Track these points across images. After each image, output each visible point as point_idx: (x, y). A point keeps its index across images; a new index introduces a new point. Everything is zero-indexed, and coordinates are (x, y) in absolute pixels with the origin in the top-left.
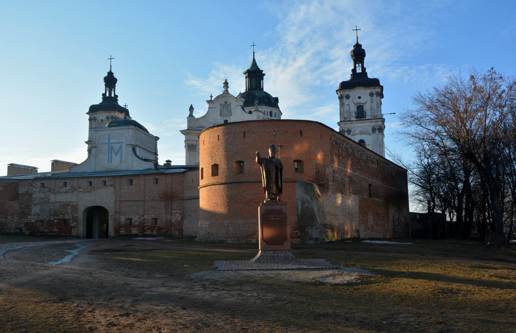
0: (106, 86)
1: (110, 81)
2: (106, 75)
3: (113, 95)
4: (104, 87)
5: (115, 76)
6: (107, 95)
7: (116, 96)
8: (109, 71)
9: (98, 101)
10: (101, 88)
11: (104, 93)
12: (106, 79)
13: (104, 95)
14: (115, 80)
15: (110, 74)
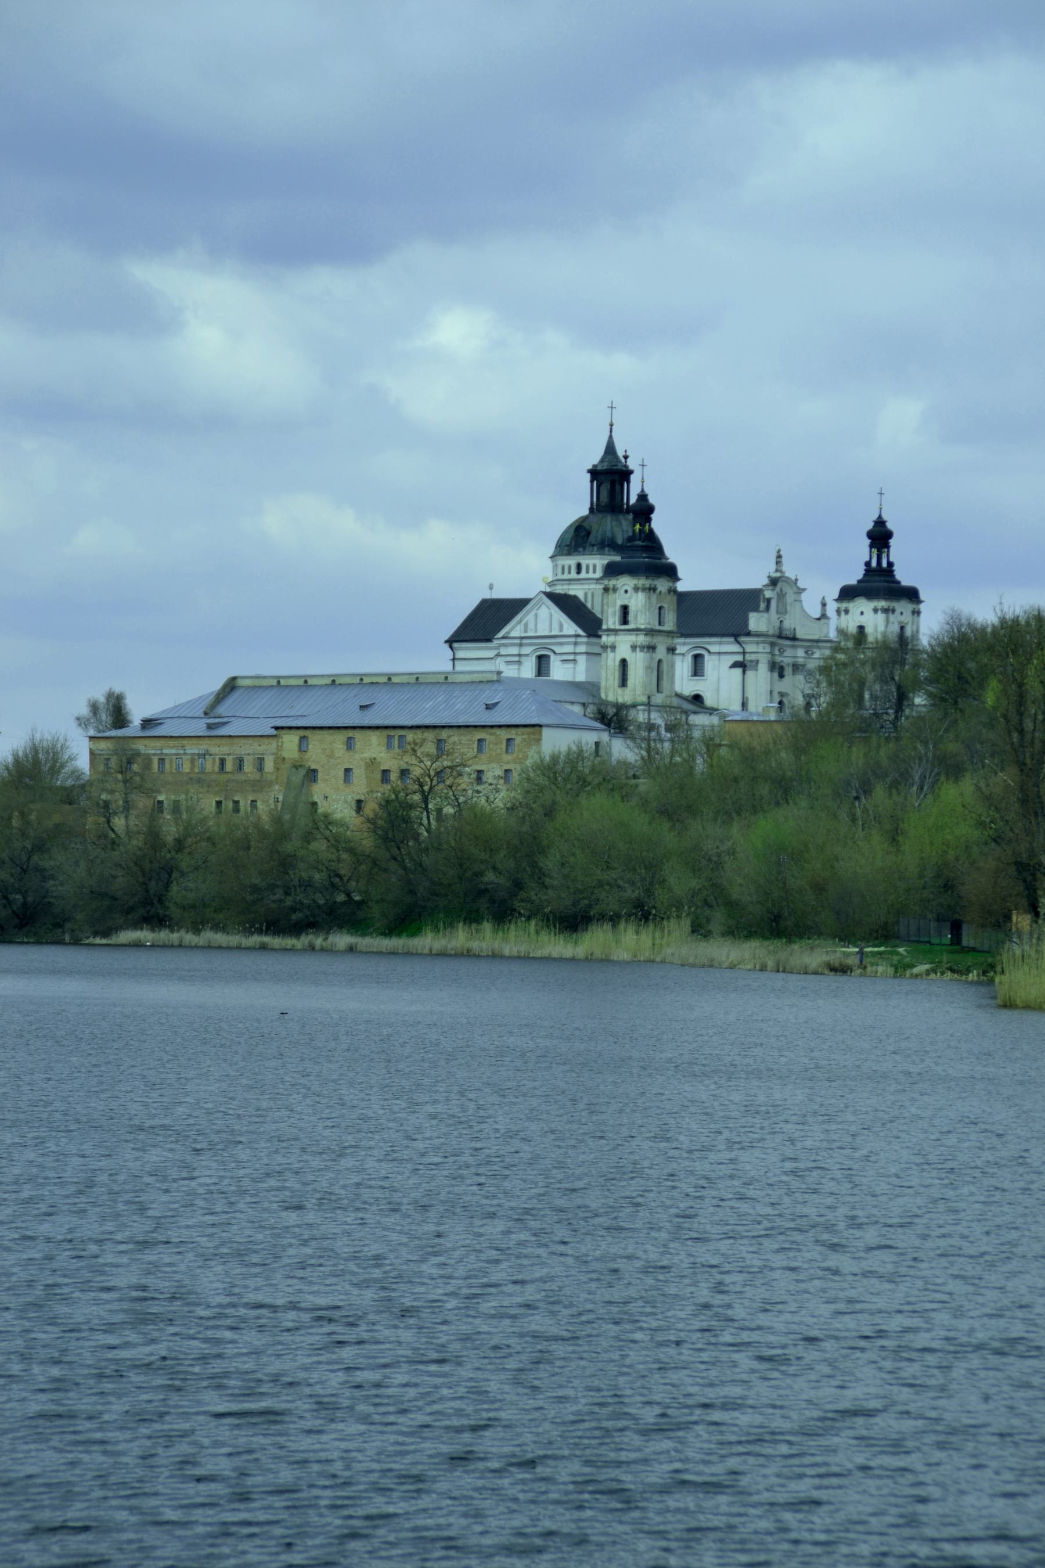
0: (871, 546)
1: (880, 537)
2: (870, 526)
3: (884, 564)
4: (867, 549)
5: (890, 526)
6: (874, 564)
7: (890, 564)
8: (875, 517)
9: (854, 575)
10: (862, 551)
11: (868, 559)
12: (870, 535)
13: (868, 564)
14: (889, 535)
15: (880, 523)
